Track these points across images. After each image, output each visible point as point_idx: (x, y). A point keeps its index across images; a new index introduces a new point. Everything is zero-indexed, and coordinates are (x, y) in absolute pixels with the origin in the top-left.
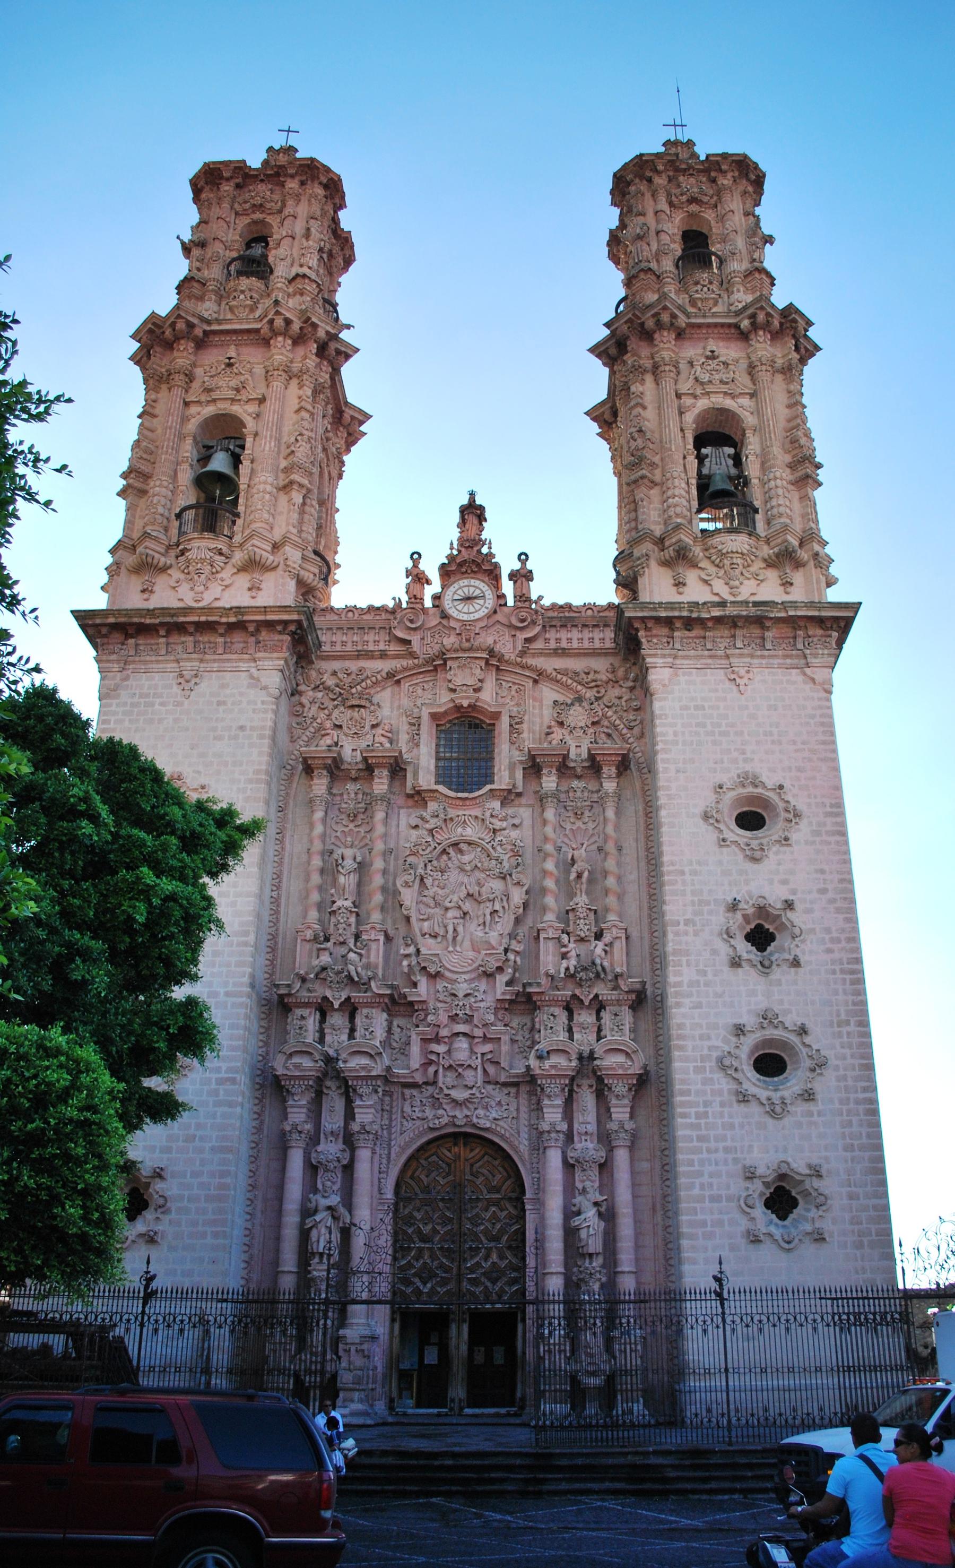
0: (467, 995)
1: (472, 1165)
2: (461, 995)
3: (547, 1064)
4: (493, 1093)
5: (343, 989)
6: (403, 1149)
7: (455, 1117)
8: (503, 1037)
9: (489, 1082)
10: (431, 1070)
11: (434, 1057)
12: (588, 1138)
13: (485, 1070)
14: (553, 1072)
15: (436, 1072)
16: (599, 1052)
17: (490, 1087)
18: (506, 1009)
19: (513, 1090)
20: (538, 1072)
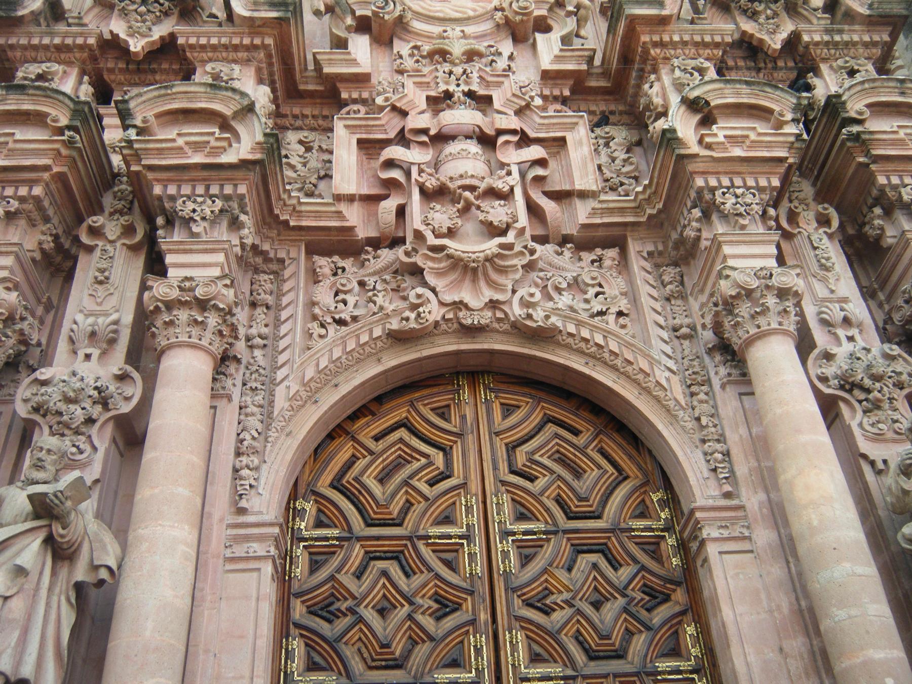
0: (471, 56)
1: (512, 448)
2: (457, 49)
3: (720, 131)
4: (557, 260)
5: (158, 21)
6: (311, 392)
7: (459, 305)
8: (569, 137)
9: (542, 240)
10: (389, 205)
11: (396, 174)
12: (854, 332)
13: (533, 210)
14: (738, 152)
15: (401, 212)
16: (855, 106)
17: (550, 248)
18: (564, 101)
19: (612, 254)
20: (695, 149)
